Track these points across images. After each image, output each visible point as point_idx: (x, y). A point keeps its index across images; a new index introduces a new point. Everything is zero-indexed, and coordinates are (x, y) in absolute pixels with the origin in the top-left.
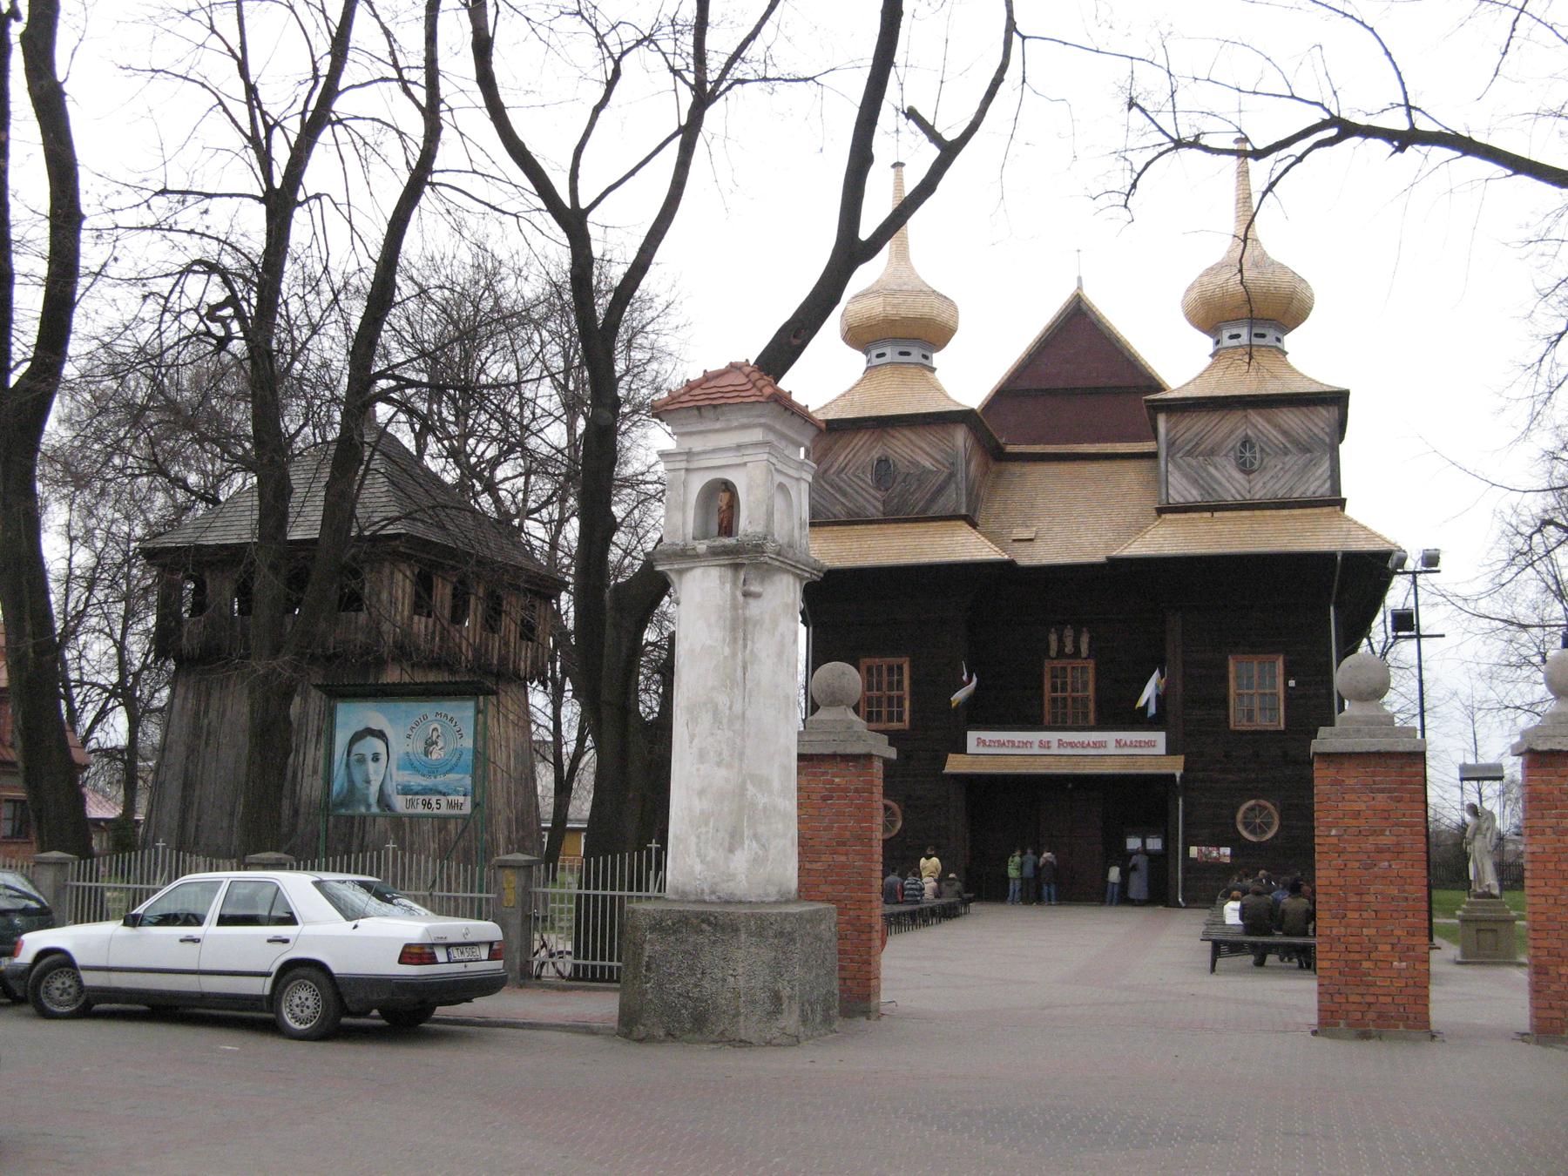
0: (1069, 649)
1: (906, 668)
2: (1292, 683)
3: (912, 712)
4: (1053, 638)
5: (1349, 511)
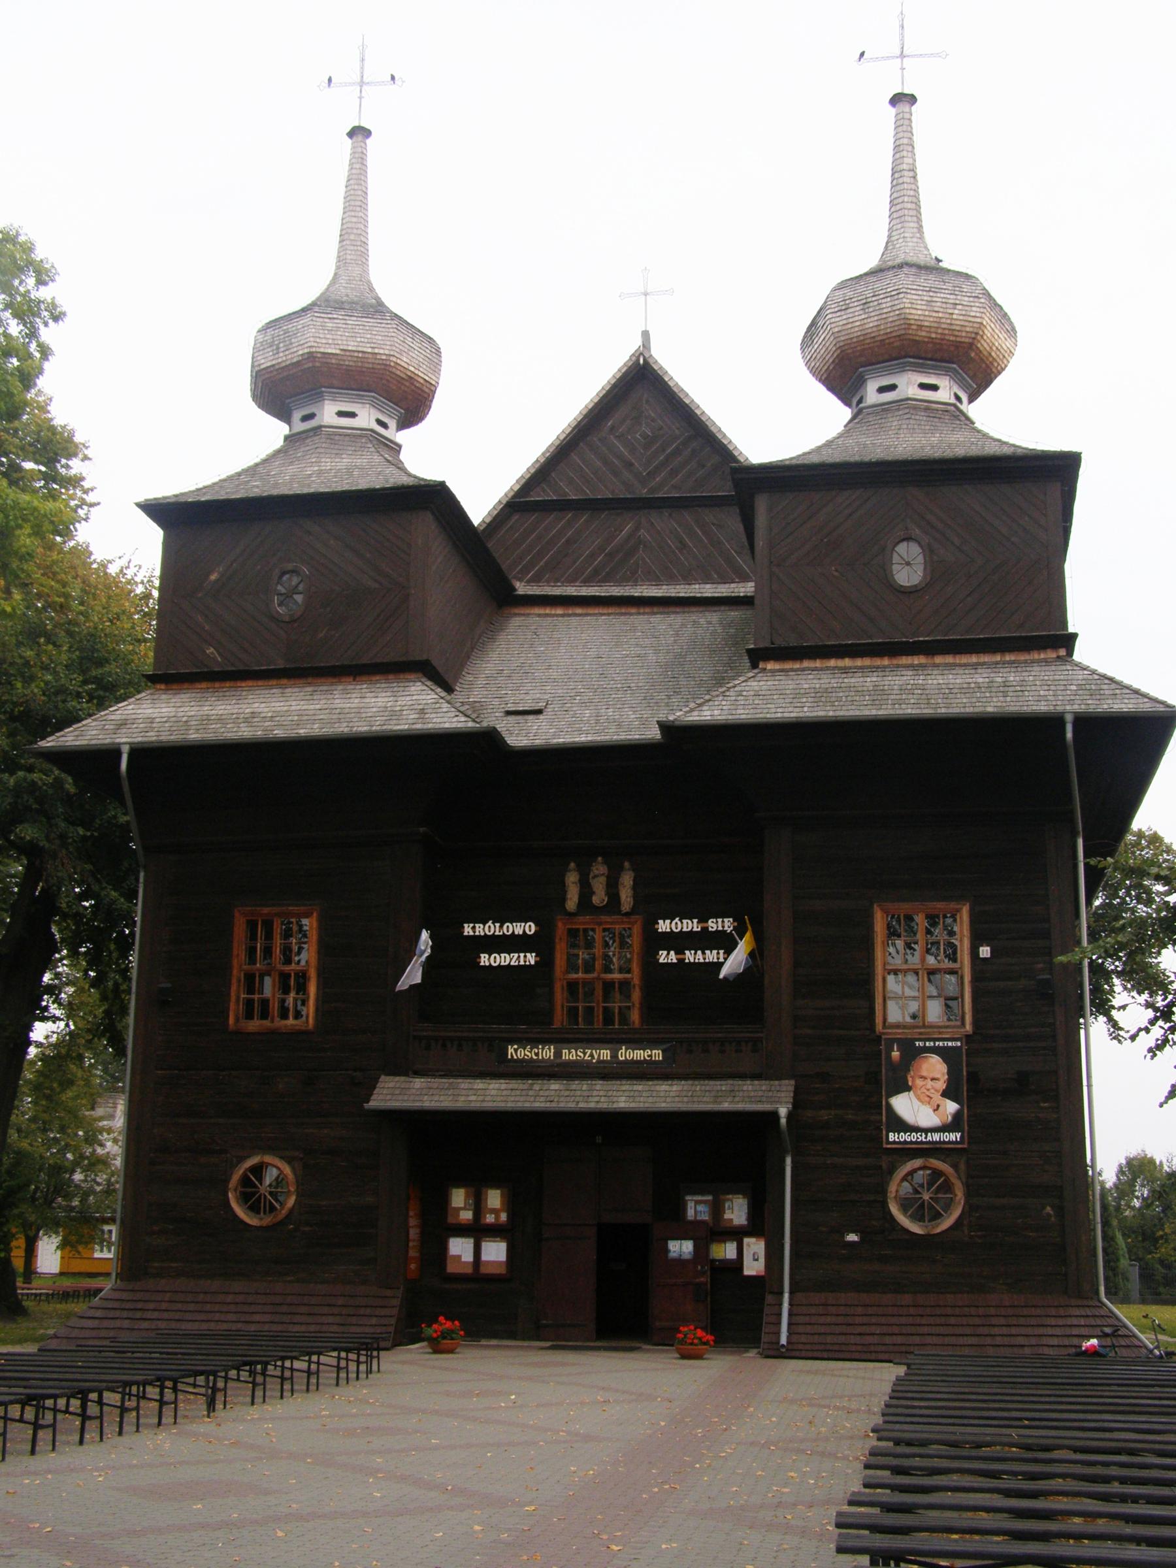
0: (599, 897)
2: (985, 952)
3: (322, 999)
4: (572, 878)
5: (1080, 653)
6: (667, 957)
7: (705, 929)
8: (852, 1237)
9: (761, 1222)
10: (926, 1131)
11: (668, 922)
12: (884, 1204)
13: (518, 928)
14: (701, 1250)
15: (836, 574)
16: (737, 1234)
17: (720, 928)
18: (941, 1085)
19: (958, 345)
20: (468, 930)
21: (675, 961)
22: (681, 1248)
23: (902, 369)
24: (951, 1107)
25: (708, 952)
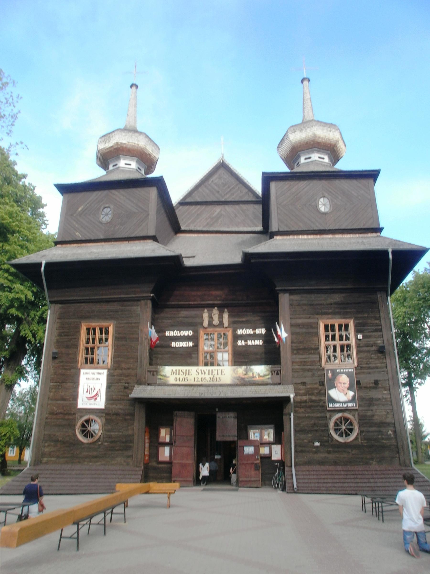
0: (216, 322)
1: (111, 329)
2: (360, 337)
6: (241, 343)
7: (246, 341)
8: (317, 444)
9: (278, 440)
10: (343, 403)
11: (241, 330)
12: (328, 430)
14: (257, 451)
15: (300, 208)
16: (269, 444)
17: (260, 332)
18: (347, 385)
19: (331, 145)
20: (167, 334)
21: (244, 344)
22: (249, 450)
23: (313, 152)
24: (351, 394)
25: (256, 341)
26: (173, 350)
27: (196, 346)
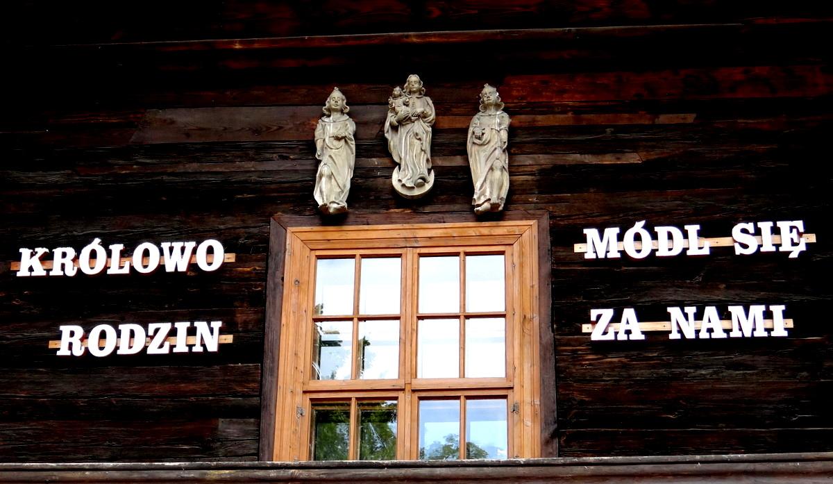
0: (412, 167)
13: (176, 257)
17: (768, 247)
20: (29, 264)
26: (66, 386)
27: (251, 350)
